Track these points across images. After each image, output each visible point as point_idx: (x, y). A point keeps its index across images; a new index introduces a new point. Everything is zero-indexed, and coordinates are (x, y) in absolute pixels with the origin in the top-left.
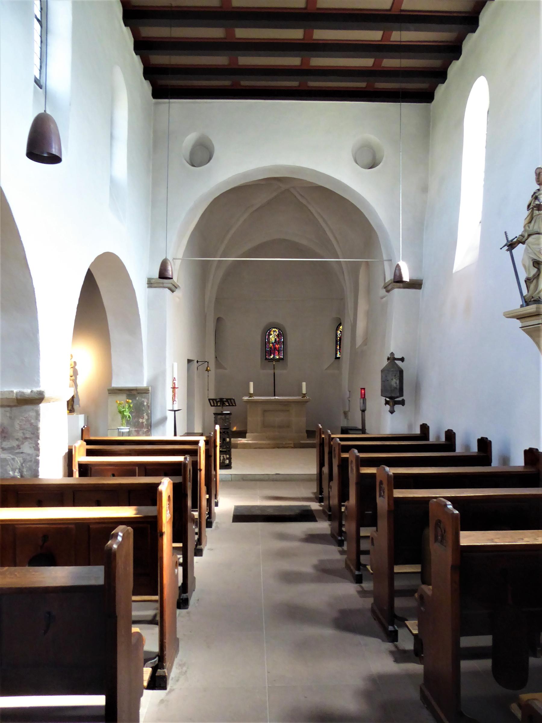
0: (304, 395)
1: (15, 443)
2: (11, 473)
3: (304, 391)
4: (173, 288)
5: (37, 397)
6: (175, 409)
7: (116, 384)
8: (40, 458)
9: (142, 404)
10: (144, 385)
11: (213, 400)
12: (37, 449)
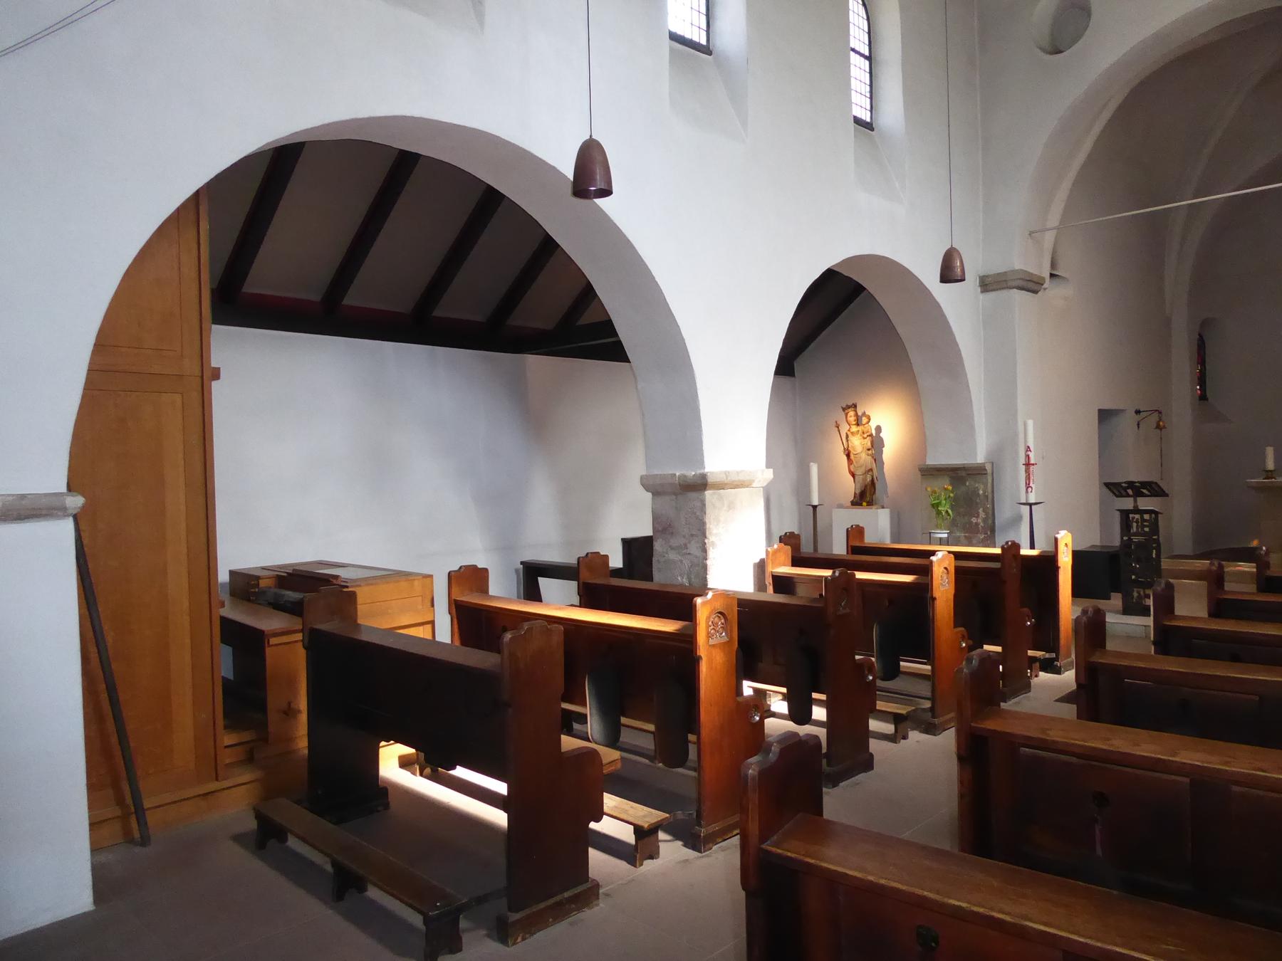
0: (1269, 474)
1: (682, 541)
3: (1270, 465)
4: (1035, 287)
6: (1032, 500)
7: (933, 460)
8: (708, 562)
9: (975, 492)
10: (980, 458)
12: (705, 551)
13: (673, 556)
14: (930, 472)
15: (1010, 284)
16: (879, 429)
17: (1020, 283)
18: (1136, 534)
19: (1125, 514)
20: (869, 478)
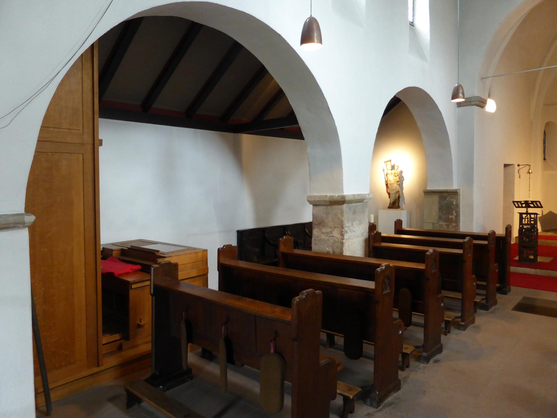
1: (329, 230)
2: (327, 249)
5: (343, 200)
11: (517, 202)
12: (343, 235)
13: (323, 237)
14: (428, 193)
15: (473, 103)
16: (401, 172)
17: (477, 103)
18: (526, 224)
19: (521, 214)
20: (397, 196)
